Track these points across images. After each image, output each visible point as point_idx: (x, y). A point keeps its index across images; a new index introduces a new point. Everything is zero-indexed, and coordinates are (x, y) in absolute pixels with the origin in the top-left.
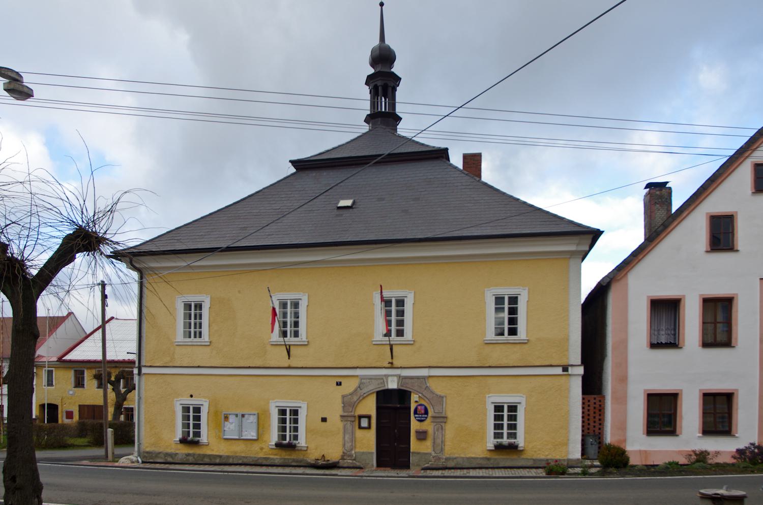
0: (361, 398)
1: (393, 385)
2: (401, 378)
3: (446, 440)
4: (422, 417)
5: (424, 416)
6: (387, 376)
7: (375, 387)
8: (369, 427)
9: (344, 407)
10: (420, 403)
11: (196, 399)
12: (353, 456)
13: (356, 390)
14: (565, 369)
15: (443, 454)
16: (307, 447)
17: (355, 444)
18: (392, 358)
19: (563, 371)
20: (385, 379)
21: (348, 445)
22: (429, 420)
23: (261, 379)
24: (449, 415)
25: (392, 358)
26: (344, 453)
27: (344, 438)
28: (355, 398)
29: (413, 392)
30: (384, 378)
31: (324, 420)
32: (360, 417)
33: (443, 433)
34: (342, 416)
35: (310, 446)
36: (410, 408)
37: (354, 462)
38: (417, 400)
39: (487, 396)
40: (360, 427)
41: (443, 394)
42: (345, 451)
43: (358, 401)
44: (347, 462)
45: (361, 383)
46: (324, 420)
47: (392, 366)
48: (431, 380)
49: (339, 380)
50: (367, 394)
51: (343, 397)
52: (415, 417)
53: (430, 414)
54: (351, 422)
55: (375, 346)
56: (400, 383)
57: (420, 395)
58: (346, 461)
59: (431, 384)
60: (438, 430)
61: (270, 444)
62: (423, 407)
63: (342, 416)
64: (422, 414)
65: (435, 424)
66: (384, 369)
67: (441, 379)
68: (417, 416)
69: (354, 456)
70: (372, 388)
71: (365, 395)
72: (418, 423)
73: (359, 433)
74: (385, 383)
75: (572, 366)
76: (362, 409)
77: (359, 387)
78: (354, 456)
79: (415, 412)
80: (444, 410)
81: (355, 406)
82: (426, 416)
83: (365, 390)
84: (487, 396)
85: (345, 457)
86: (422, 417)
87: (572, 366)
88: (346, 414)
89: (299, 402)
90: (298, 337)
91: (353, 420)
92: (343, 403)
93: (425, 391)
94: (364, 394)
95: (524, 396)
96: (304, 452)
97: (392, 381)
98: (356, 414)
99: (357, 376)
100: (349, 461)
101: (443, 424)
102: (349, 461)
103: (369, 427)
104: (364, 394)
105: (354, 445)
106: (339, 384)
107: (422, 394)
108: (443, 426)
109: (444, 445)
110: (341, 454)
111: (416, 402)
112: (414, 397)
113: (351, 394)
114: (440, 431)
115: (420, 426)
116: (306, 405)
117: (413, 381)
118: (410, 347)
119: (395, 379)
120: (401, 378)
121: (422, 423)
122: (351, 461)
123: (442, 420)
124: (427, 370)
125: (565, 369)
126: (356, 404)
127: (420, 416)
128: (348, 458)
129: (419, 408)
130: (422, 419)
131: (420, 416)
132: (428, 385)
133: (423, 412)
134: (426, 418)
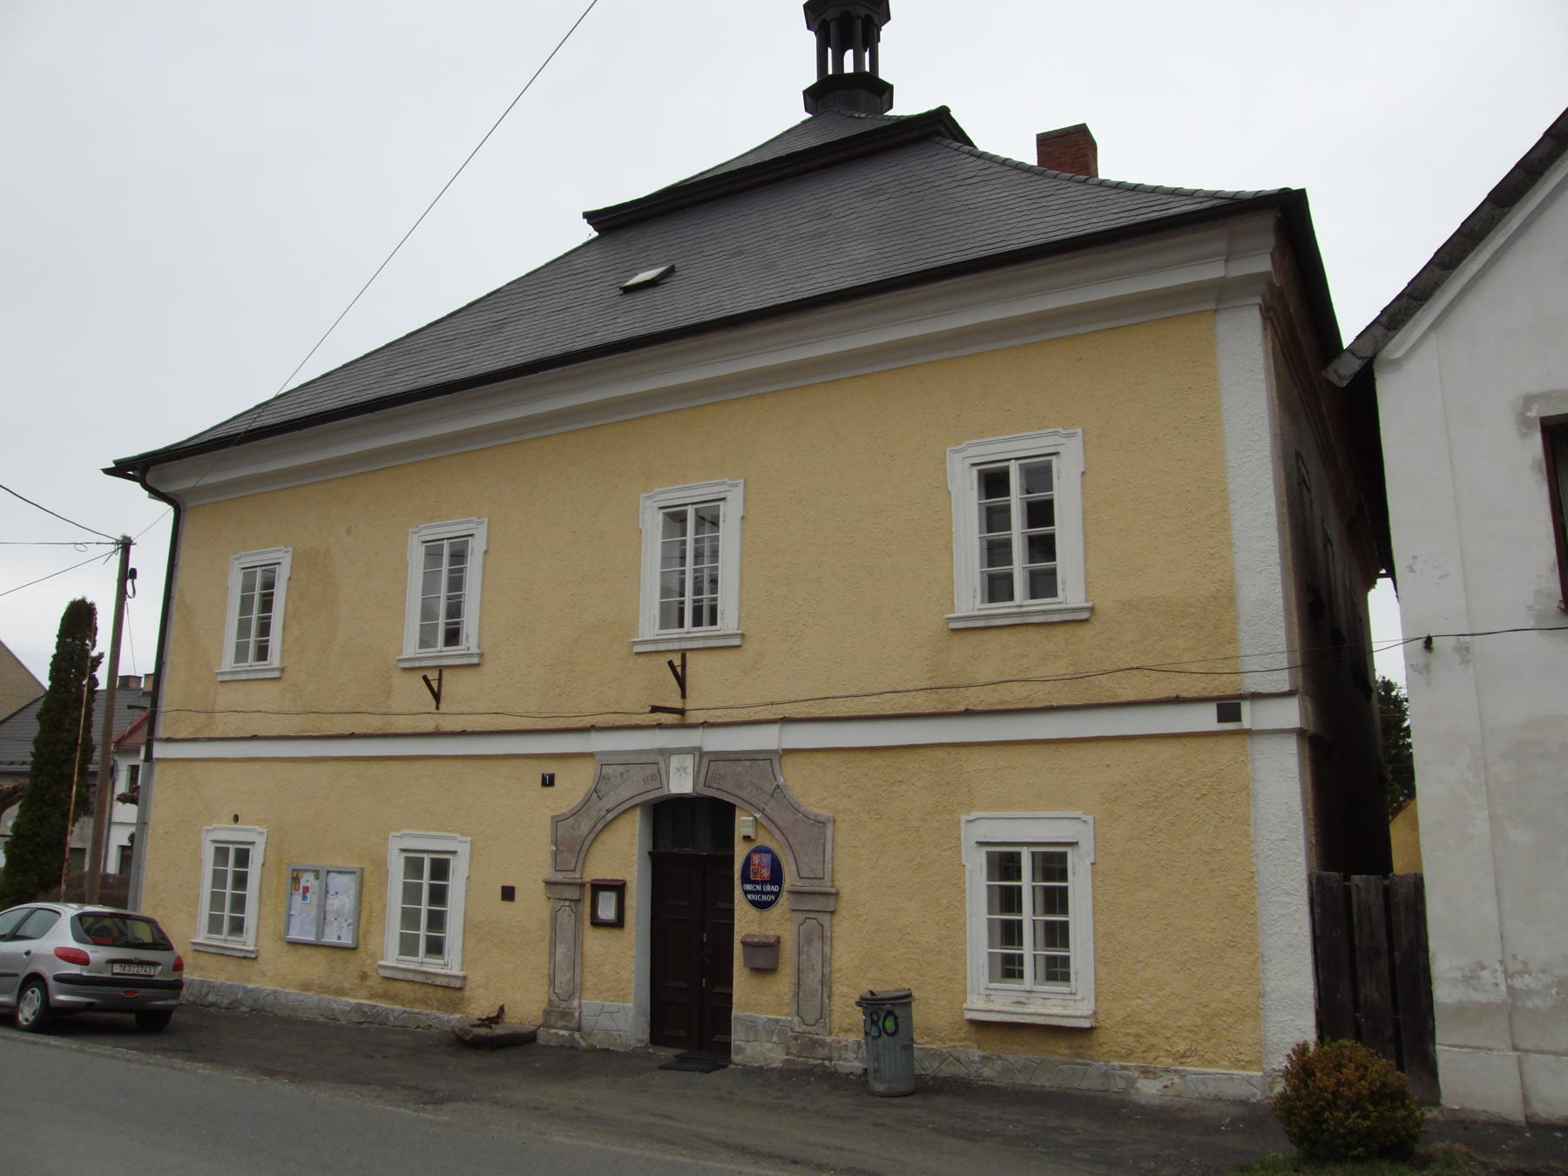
0: (600, 826)
1: (681, 783)
2: (705, 760)
3: (836, 975)
4: (762, 892)
5: (768, 888)
6: (666, 753)
7: (634, 788)
8: (619, 923)
9: (555, 854)
10: (758, 844)
11: (244, 827)
12: (572, 1014)
13: (587, 800)
14: (1229, 710)
15: (825, 1026)
16: (465, 978)
17: (581, 977)
18: (684, 696)
19: (1221, 719)
20: (662, 765)
21: (563, 978)
22: (784, 901)
23: (377, 769)
24: (845, 885)
25: (684, 696)
26: (550, 1001)
27: (552, 954)
28: (585, 827)
29: (741, 809)
30: (661, 760)
31: (508, 894)
32: (598, 887)
33: (827, 949)
34: (549, 884)
35: (470, 977)
36: (730, 860)
37: (577, 1035)
38: (749, 831)
39: (964, 818)
40: (597, 923)
41: (823, 813)
42: (554, 998)
43: (592, 836)
44: (557, 1034)
45: (601, 778)
46: (508, 894)
47: (680, 718)
48: (788, 762)
49: (549, 768)
50: (615, 813)
51: (557, 821)
52: (746, 892)
53: (787, 885)
54: (573, 904)
55: (641, 659)
56: (702, 779)
57: (758, 816)
58: (553, 1031)
59: (793, 777)
60: (809, 942)
61: (381, 963)
62: (766, 859)
63: (549, 884)
64: (763, 882)
65: (802, 916)
66: (658, 732)
67: (819, 757)
68: (749, 887)
69: (577, 1015)
70: (629, 795)
71: (610, 816)
72: (753, 912)
73: (594, 941)
74: (664, 775)
75: (1255, 696)
76: (600, 867)
77: (595, 790)
78: (577, 1015)
79: (746, 879)
80: (828, 866)
81: (585, 848)
82: (775, 888)
83: (610, 801)
84: (964, 818)
85: (553, 1019)
86: (762, 892)
87: (1255, 696)
88: (559, 877)
89: (454, 839)
90: (265, 659)
91: (576, 897)
92: (555, 842)
93: (773, 803)
94: (608, 811)
95: (1084, 818)
96: (458, 994)
97: (678, 770)
98: (588, 878)
99: (591, 755)
100: (562, 1032)
101: (825, 919)
102: (562, 1032)
103: (619, 923)
104: (608, 811)
105: (577, 978)
106: (548, 781)
107: (762, 811)
108: (827, 926)
109: (829, 997)
110: (544, 1005)
111: (747, 838)
112: (743, 824)
113: (576, 813)
114: (817, 944)
115: (760, 925)
116: (468, 845)
117: (739, 767)
118: (731, 656)
119: (689, 762)
120: (705, 760)
121: (766, 913)
122: (566, 1033)
123: (819, 904)
124: (775, 729)
125: (1229, 710)
126: (587, 843)
127: (759, 888)
128: (561, 1023)
129: (756, 859)
130: (764, 898)
131: (759, 888)
132: (781, 781)
133: (766, 873)
134: (777, 894)
